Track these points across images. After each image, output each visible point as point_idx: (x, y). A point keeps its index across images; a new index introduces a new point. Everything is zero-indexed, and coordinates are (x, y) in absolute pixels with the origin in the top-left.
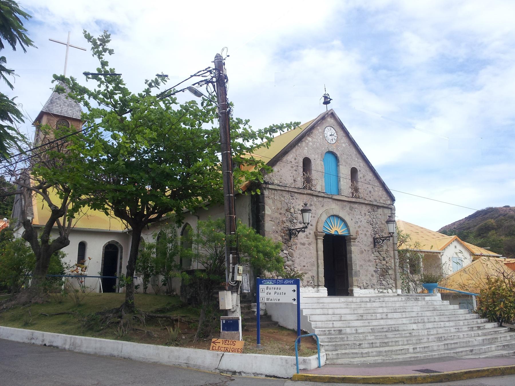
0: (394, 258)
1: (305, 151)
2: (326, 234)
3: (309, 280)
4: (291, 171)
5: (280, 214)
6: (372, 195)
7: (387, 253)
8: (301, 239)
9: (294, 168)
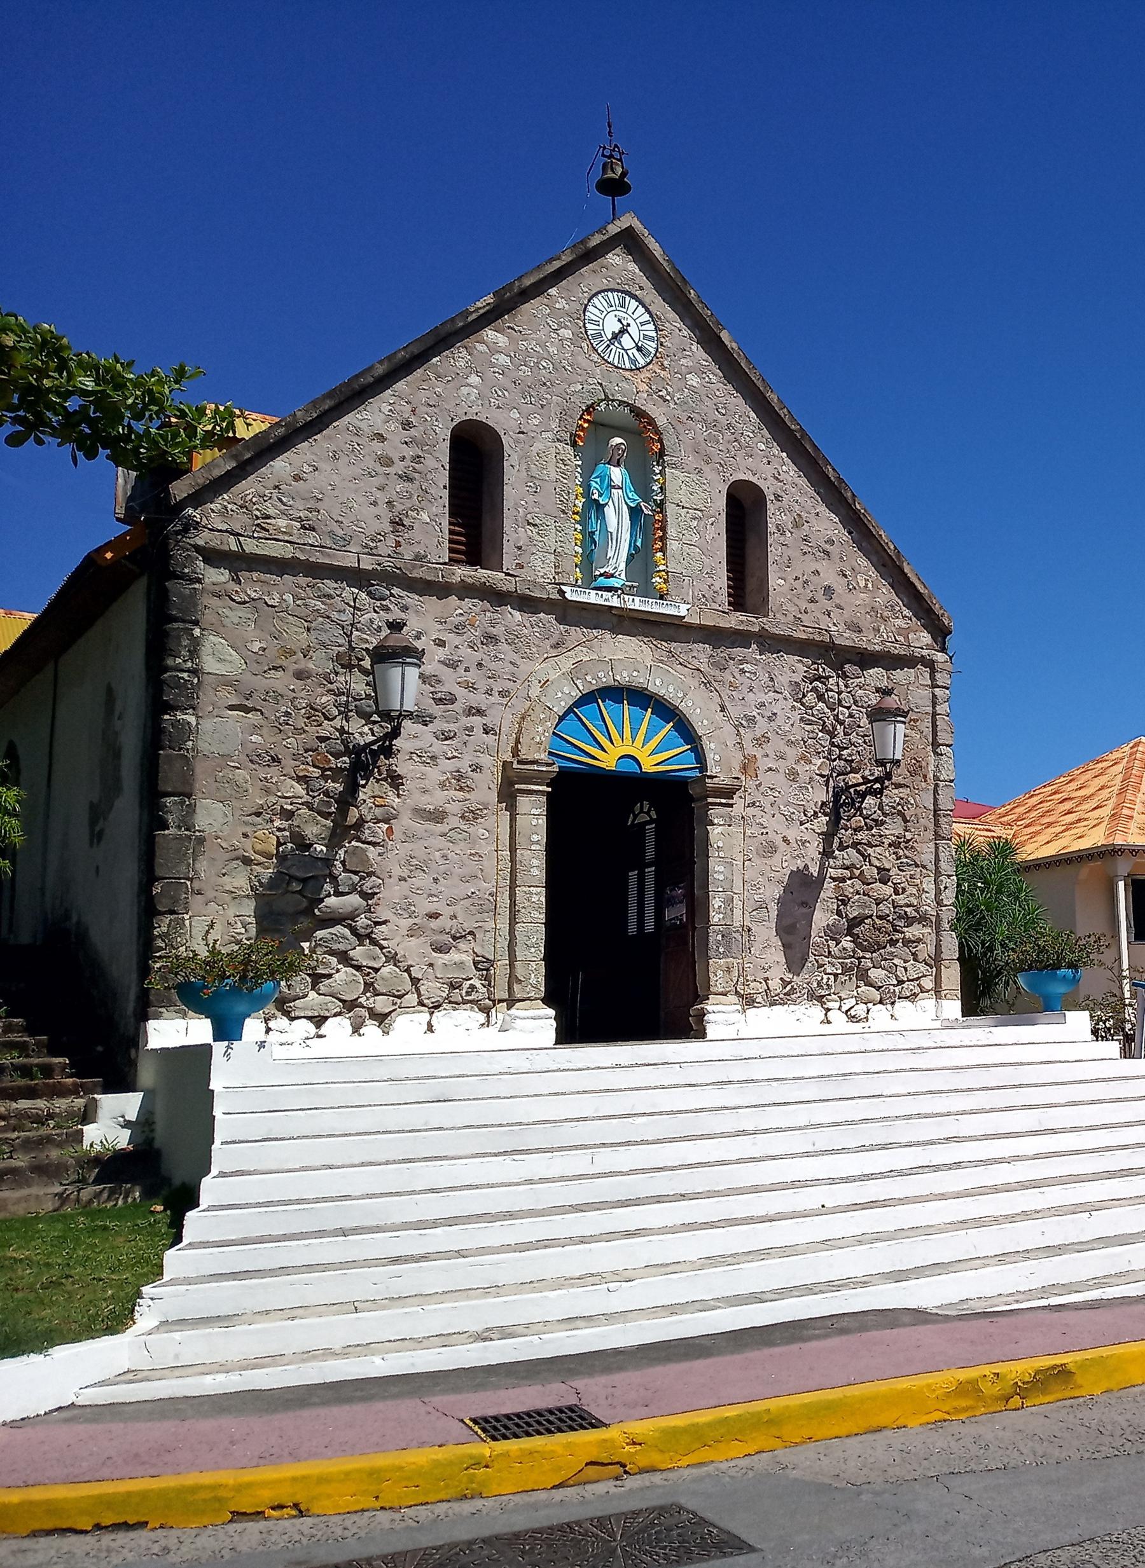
1: (465, 390)
2: (563, 772)
4: (377, 481)
5: (300, 675)
6: (839, 607)
7: (901, 853)
8: (425, 791)
9: (399, 467)
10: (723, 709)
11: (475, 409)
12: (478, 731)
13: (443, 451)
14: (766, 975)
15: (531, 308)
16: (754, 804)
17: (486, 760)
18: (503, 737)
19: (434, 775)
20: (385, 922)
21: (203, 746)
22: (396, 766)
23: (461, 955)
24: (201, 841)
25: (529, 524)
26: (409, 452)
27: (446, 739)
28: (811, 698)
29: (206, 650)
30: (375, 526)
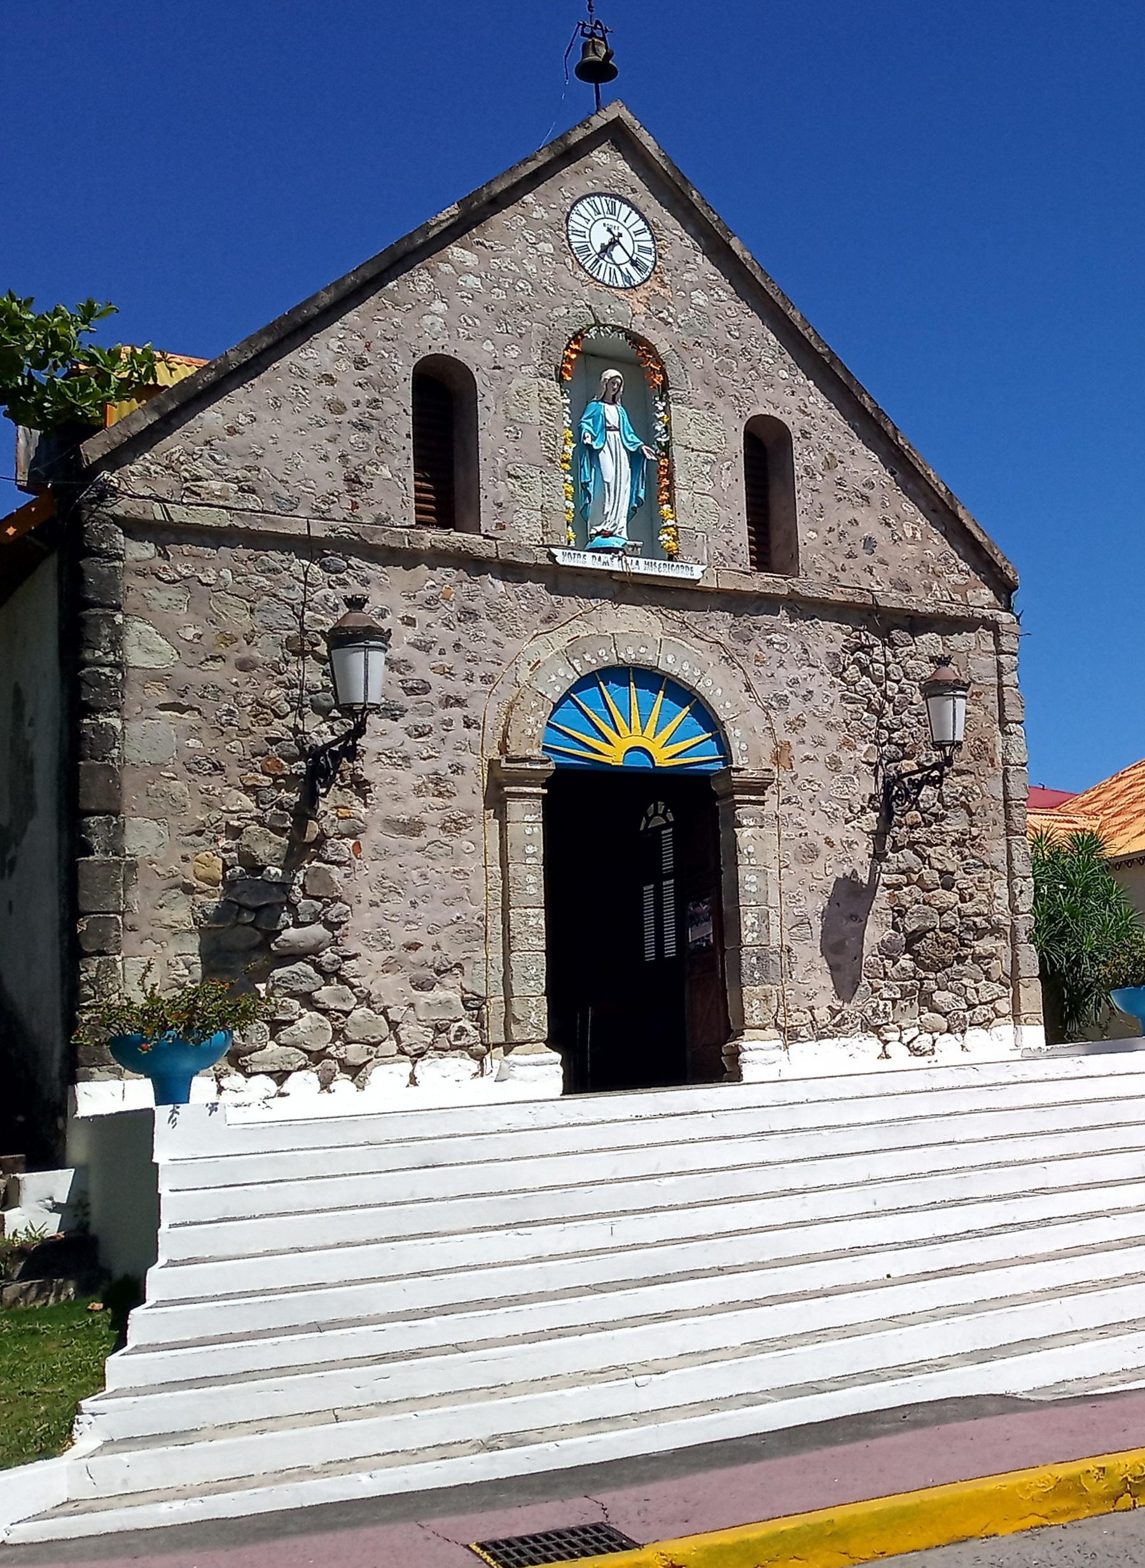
0: (1011, 875)
1: (428, 320)
2: (560, 770)
3: (443, 1016)
4: (327, 432)
5: (244, 666)
6: (882, 562)
7: (967, 852)
8: (397, 799)
9: (353, 414)
10: (749, 688)
11: (441, 341)
12: (458, 724)
13: (405, 392)
14: (811, 1003)
15: (500, 219)
16: (789, 799)
17: (468, 759)
18: (488, 731)
19: (407, 778)
20: (355, 956)
21: (130, 754)
22: (362, 770)
23: (448, 992)
24: (133, 867)
25: (510, 476)
26: (364, 396)
27: (420, 736)
28: (853, 671)
29: (130, 640)
30: (326, 486)
